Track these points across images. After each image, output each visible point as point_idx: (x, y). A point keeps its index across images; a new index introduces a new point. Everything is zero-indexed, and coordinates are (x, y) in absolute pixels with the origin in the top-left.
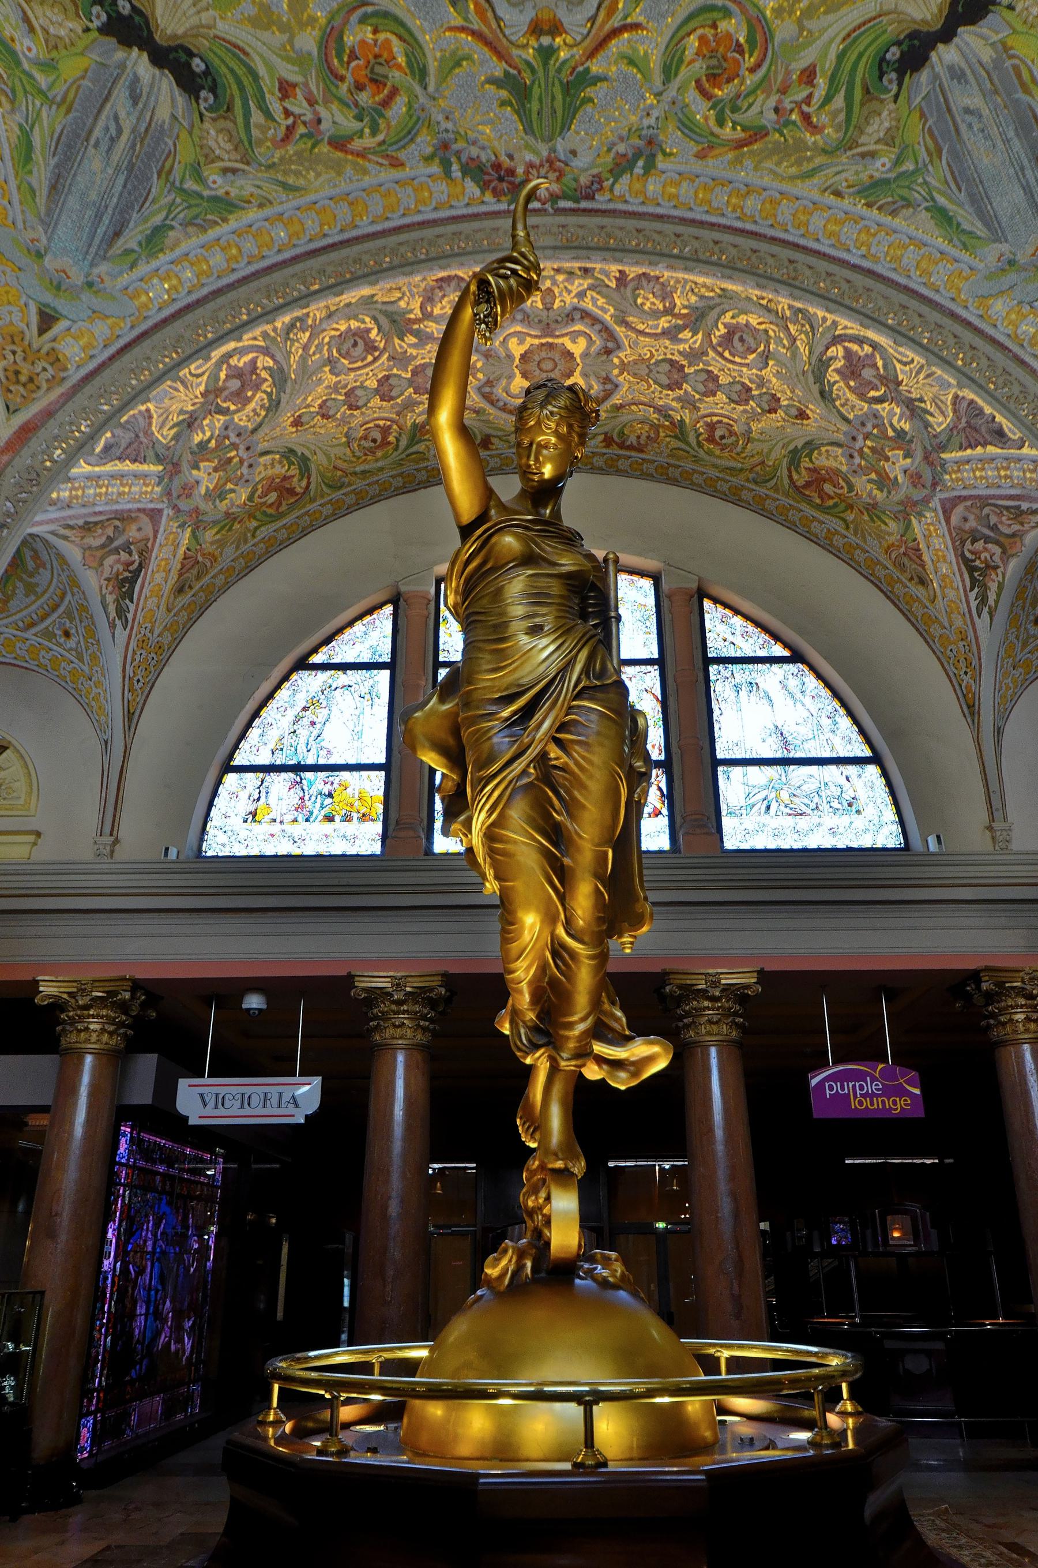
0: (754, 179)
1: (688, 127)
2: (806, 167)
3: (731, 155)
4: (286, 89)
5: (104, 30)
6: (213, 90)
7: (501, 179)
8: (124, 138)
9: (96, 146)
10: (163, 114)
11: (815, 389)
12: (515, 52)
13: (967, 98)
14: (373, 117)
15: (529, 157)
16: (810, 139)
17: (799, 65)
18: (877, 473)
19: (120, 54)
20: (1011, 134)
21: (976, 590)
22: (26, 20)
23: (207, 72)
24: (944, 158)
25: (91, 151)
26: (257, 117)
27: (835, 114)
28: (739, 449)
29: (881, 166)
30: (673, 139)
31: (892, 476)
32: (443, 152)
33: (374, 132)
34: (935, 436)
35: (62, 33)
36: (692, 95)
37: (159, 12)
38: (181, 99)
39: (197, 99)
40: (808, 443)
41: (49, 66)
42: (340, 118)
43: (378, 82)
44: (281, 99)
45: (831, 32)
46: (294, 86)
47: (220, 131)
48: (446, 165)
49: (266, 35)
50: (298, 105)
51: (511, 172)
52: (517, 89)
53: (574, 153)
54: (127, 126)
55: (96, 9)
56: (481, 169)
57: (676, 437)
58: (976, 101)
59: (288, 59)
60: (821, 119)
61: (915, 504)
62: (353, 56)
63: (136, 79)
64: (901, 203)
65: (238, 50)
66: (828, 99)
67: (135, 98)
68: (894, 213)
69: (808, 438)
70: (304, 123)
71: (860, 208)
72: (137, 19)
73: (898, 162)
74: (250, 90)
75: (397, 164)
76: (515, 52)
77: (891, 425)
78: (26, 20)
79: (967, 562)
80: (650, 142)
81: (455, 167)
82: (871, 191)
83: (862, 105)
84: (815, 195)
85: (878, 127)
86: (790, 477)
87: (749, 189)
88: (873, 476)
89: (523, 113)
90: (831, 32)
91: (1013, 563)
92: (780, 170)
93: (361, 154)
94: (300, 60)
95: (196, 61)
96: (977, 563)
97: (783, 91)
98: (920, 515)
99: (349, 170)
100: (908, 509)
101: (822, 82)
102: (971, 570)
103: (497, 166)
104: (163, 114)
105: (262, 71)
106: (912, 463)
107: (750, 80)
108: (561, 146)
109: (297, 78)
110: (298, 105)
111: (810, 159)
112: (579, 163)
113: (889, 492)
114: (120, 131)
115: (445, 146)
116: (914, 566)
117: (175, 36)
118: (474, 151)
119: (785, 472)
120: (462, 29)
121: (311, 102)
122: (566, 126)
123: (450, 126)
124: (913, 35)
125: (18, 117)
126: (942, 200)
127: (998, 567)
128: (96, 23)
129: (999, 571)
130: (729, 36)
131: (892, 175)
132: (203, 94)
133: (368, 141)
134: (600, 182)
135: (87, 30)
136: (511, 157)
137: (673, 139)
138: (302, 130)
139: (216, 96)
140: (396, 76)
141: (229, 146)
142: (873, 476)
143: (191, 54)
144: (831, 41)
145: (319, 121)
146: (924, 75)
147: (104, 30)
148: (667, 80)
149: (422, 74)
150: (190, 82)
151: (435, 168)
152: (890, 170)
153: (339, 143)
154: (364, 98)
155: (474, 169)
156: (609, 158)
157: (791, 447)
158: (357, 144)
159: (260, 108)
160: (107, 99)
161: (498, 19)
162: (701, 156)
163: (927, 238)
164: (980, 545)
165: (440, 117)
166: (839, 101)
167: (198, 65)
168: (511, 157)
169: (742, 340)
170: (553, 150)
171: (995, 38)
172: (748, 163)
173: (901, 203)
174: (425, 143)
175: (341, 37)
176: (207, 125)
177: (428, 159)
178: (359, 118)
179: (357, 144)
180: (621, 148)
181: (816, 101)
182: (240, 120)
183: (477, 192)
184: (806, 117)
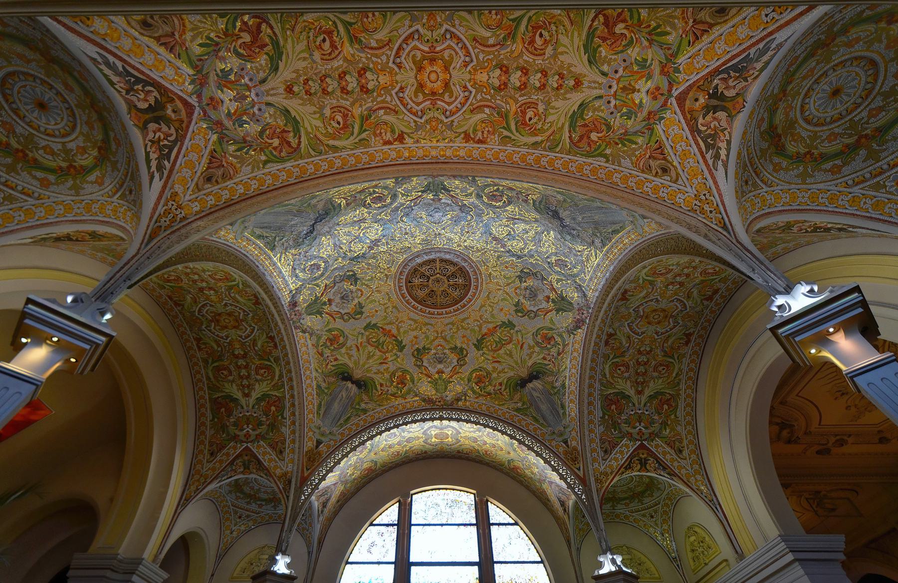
11: (293, 114)
18: (233, 82)
21: (121, 69)
28: (311, 34)
31: (225, 89)
34: (228, 142)
40: (277, 69)
57: (351, 24)
61: (202, 85)
69: (279, 73)
77: (249, 124)
79: (146, 83)
86: (272, 28)
88: (232, 77)
91: (123, 107)
96: (140, 87)
98: (192, 82)
100: (201, 81)
102: (138, 81)
106: (224, 112)
113: (217, 75)
116: (160, 32)
119: (277, 31)
127: (127, 94)
129: (124, 92)
142: (232, 77)
157: (284, 57)
164: (152, 101)
169: (339, 123)
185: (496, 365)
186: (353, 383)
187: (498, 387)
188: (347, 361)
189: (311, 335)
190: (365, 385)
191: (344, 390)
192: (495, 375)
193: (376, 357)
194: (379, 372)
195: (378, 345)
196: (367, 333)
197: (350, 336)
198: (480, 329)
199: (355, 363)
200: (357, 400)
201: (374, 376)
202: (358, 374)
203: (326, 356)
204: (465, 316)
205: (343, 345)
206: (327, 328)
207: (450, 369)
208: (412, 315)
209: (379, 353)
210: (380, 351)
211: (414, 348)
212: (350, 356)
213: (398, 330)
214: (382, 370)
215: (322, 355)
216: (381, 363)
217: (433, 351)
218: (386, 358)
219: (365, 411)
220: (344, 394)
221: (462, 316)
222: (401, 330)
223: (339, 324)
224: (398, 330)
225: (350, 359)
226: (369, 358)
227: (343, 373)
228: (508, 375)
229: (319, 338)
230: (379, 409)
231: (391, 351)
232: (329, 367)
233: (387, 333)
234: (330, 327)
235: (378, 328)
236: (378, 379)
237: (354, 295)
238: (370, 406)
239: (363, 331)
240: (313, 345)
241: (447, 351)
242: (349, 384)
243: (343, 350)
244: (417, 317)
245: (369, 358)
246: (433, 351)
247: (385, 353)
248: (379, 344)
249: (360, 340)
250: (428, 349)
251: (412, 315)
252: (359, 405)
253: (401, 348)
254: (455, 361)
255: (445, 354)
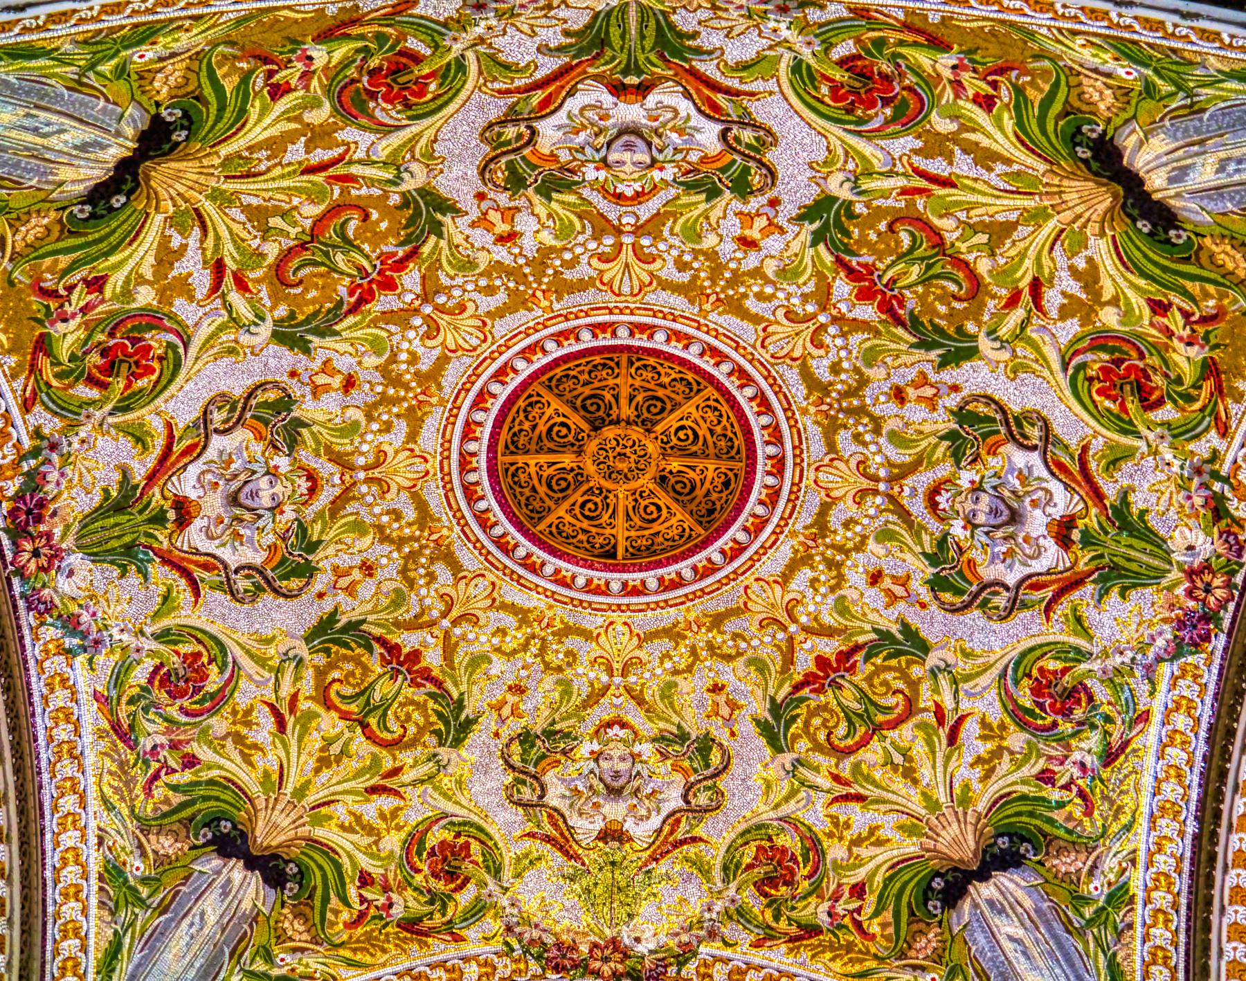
0: (90, 759)
1: (119, 677)
2: (115, 799)
3: (107, 726)
4: (95, 285)
5: (156, 119)
6: (93, 216)
7: (29, 512)
8: (38, 140)
9: (27, 115)
10: (65, 173)
12: (156, 490)
13: (212, 908)
14: (74, 373)
15: (57, 532)
16: (138, 790)
17: (196, 749)
19: (130, 132)
20: (197, 965)
22: (173, 55)
23: (111, 209)
24: (162, 918)
25: (21, 112)
26: (64, 261)
27: (167, 801)
29: (136, 867)
30: (106, 661)
32: (45, 445)
33: (56, 376)
35: (157, 84)
36: (149, 664)
37: (173, 165)
38: (80, 188)
39: (83, 203)
41: (121, 72)
42: (70, 339)
43: (109, 369)
44: (84, 280)
45: (228, 764)
46: (100, 290)
47: (48, 229)
48: (35, 452)
49: (151, 259)
50: (79, 298)
51: (39, 519)
52: (123, 501)
53: (71, 573)
54: (53, 142)
55: (179, 113)
56: (38, 488)
58: (211, 919)
59: (127, 281)
60: (159, 791)
62: (134, 341)
63: (103, 147)
64: (111, 904)
65: (135, 234)
66: (175, 788)
67: (83, 147)
68: (102, 904)
70: (62, 306)
71: (95, 868)
72: (167, 147)
73: (145, 880)
74: (94, 249)
75: (27, 406)
76: (156, 490)
78: (173, 55)
80: (97, 642)
81: (33, 462)
82: (113, 872)
83: (179, 821)
84: (93, 824)
85: (166, 845)
87: (77, 758)
89: (100, 512)
90: (228, 764)
92: (106, 777)
93: (33, 368)
94: (127, 293)
95: (123, 199)
97: (174, 746)
99: (12, 360)
101: (187, 776)
103: (42, 504)
104: (65, 173)
105: (113, 259)
107: (173, 711)
108: (75, 559)
109: (108, 292)
110: (79, 298)
111: (122, 799)
112: (65, 585)
114: (45, 136)
115: (53, 447)
117: (148, 179)
118: (53, 476)
120: (171, 437)
121: (85, 310)
122: (95, 557)
123: (76, 445)
124: (243, 835)
125: (67, 47)
126: (127, 940)
128: (164, 113)
130: (204, 677)
131: (132, 882)
132: (88, 208)
133: (48, 372)
134: (48, 611)
135: (158, 104)
136: (54, 514)
137: (106, 661)
138: (53, 305)
139: (86, 220)
140: (119, 384)
141: (30, 238)
143: (129, 194)
144: (221, 768)
145: (65, 320)
146: (217, 862)
147: (156, 119)
148: (157, 637)
149: (124, 407)
150: (99, 195)
151: (27, 443)
152: (135, 877)
153: (43, 345)
154: (95, 359)
155: (35, 480)
156: (74, 609)
158: (44, 362)
159: (74, 262)
160: (81, 121)
161: (185, 467)
162: (96, 696)
163: (92, 949)
165: (82, 435)
166: (177, 799)
167: (118, 201)
168: (54, 514)
170: (69, 552)
171: (259, 905)
172: (104, 745)
173: (111, 904)
174: (52, 426)
175: (150, 328)
176: (53, 214)
177: (37, 433)
178: (73, 358)
179: (44, 362)
180: (85, 617)
181: (175, 779)
182: (61, 245)
183: (10, 493)
184: (156, 776)
185: (1053, 299)
186: (983, 875)
187: (1176, 321)
188: (885, 856)
189: (712, 935)
190: (1017, 836)
191: (996, 921)
192: (1109, 318)
193: (919, 749)
194: (988, 765)
195: (869, 722)
196: (803, 744)
197: (785, 810)
198: (863, 326)
199: (911, 831)
200: (1062, 899)
201: (995, 788)
202: (959, 841)
203: (823, 919)
204: (792, 375)
205: (813, 845)
206: (717, 874)
207: (1055, 487)
208: (772, 564)
209: (906, 732)
210: (894, 725)
211: (925, 594)
212: (872, 837)
213: (829, 632)
214: (984, 748)
215: (811, 930)
216: (952, 738)
217: (957, 529)
218: (939, 713)
219: (1119, 896)
220: (1007, 928)
221: (798, 391)
222: (828, 619)
223: (718, 836)
224: (829, 632)
225: (879, 843)
226: (909, 774)
227: (926, 892)
228: (1108, 264)
229: (740, 914)
230: (1141, 840)
231: (914, 685)
232: (875, 929)
233: (827, 672)
234: (718, 864)
235: (794, 699)
236: (1013, 777)
237: (617, 750)
238: (1110, 864)
239: (787, 758)
240: (757, 945)
241: (966, 478)
242: (984, 891)
243: (835, 851)
244: (785, 551)
245: (909, 774)
246: (957, 529)
247: (911, 708)
248: (865, 717)
249: (824, 781)
250: (942, 543)
251: (772, 564)
252: (1087, 900)
253: (913, 643)
254: (1020, 459)
255: (977, 488)
